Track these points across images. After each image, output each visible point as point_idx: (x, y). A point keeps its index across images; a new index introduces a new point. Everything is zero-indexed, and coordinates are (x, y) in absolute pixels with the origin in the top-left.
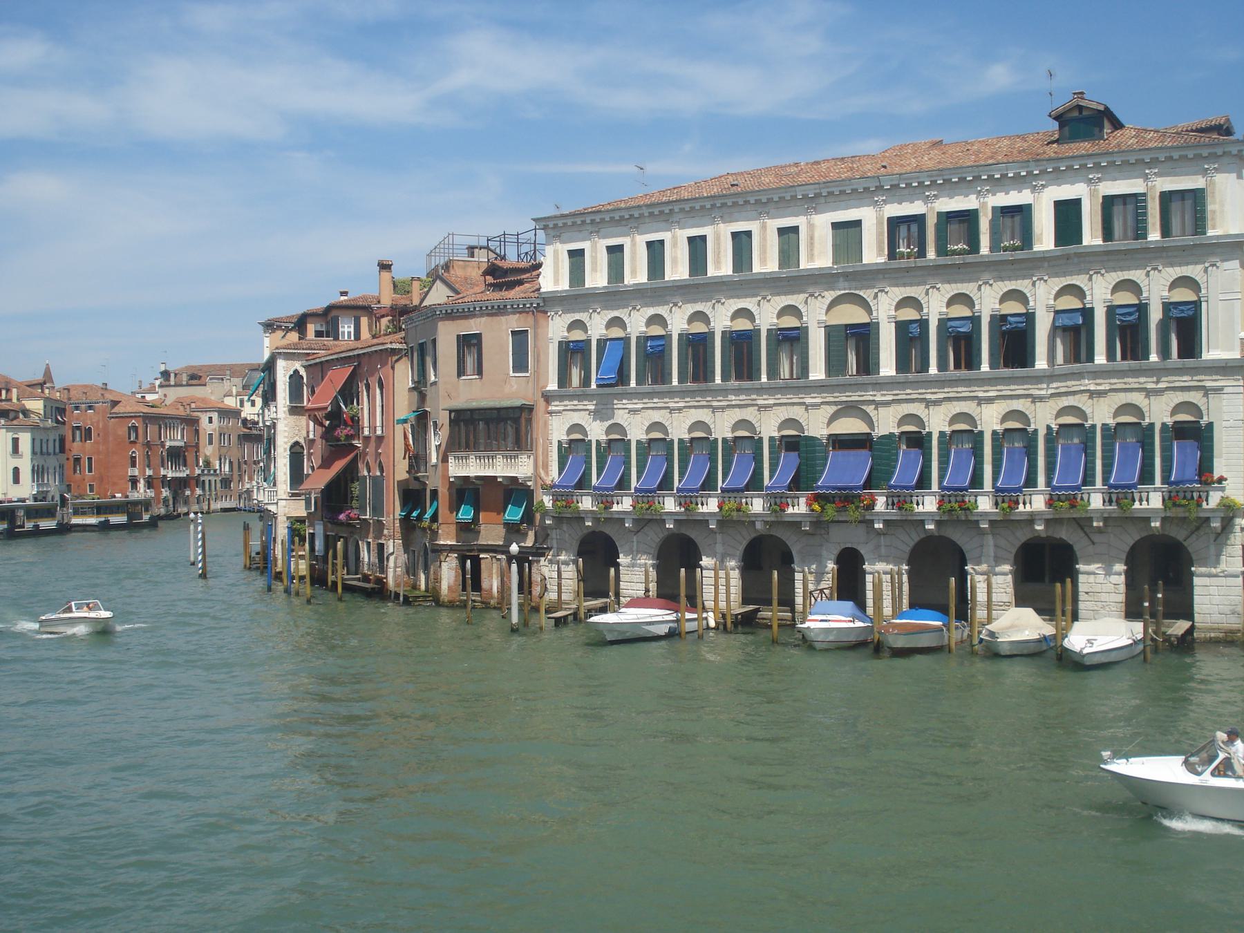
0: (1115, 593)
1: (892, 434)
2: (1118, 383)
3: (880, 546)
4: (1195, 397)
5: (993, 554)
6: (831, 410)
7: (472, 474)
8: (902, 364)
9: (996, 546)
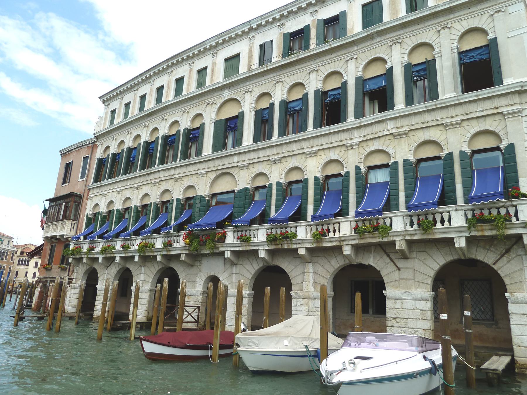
0: (422, 319)
1: (246, 189)
2: (415, 121)
3: (233, 274)
4: (489, 125)
5: (312, 281)
6: (212, 176)
7: (49, 235)
8: (257, 138)
9: (315, 273)
